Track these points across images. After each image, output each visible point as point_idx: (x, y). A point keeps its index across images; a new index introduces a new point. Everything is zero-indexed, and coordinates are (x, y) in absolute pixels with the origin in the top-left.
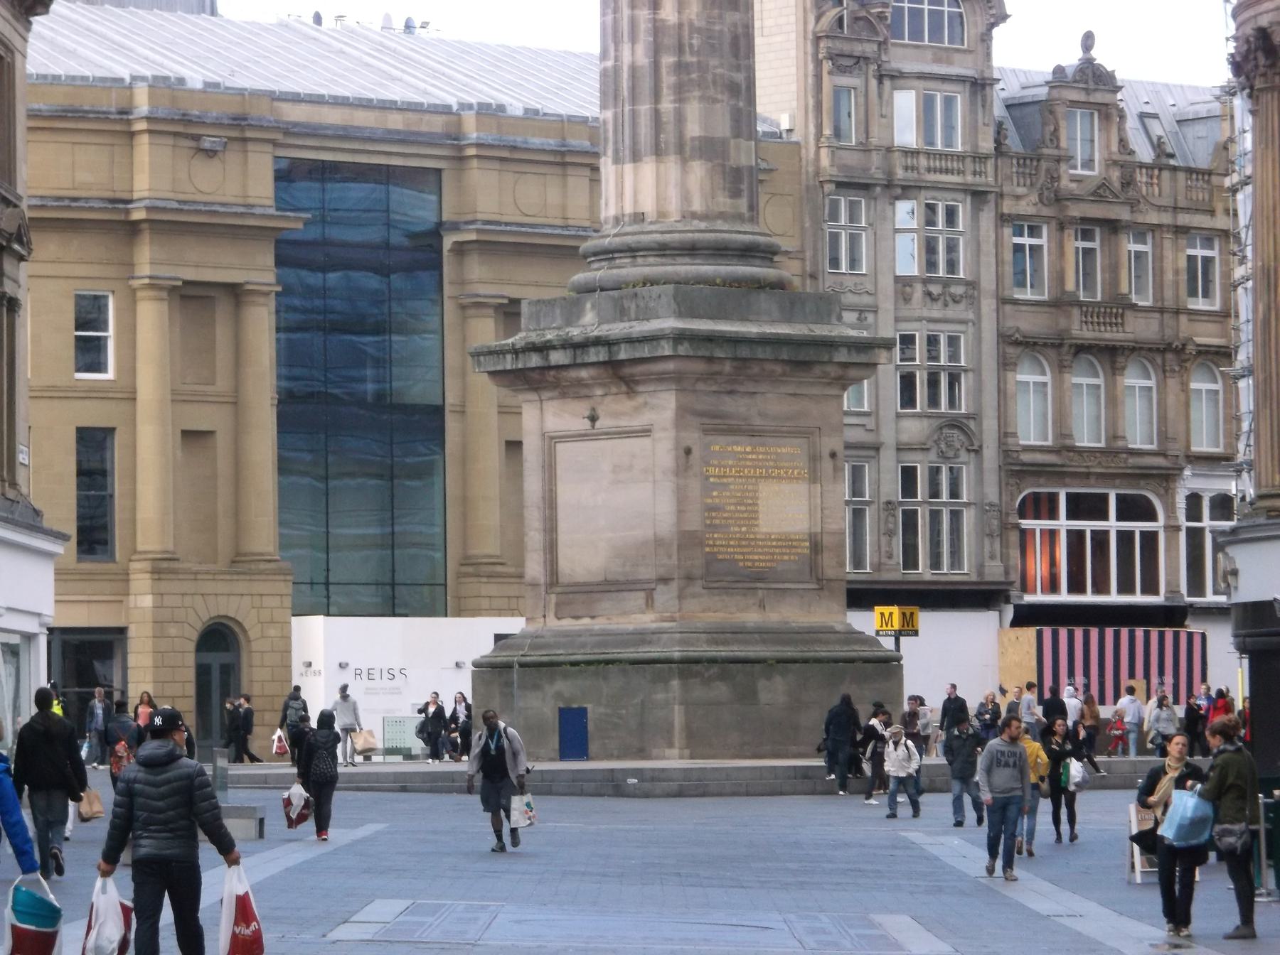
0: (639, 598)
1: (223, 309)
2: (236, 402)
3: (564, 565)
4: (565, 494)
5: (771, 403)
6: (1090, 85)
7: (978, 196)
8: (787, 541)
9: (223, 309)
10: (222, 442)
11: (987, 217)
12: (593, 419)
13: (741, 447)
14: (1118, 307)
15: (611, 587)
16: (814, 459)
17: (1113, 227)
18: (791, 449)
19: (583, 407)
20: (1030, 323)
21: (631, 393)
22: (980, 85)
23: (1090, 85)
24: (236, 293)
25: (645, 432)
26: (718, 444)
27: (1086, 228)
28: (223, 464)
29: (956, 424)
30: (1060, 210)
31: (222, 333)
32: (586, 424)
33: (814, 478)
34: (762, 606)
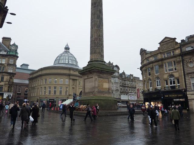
0: (91, 93)
1: (75, 81)
2: (76, 86)
3: (85, 91)
4: (86, 84)
5: (105, 75)
6: (124, 73)
7: (119, 78)
8: (106, 88)
9: (75, 81)
10: (75, 88)
11: (119, 79)
12: (88, 77)
13: (102, 79)
14: (126, 84)
15: (89, 93)
16: (109, 81)
17: (125, 80)
18: (107, 80)
19: (87, 76)
20: (121, 85)
21: (91, 74)
22: (119, 73)
23: (124, 73)
24: (76, 80)
25: (92, 77)
26: (99, 79)
27: (124, 80)
28: (75, 90)
29: (118, 90)
30: (123, 79)
31: (75, 82)
32: (87, 77)
33: (109, 83)
34: (104, 94)
